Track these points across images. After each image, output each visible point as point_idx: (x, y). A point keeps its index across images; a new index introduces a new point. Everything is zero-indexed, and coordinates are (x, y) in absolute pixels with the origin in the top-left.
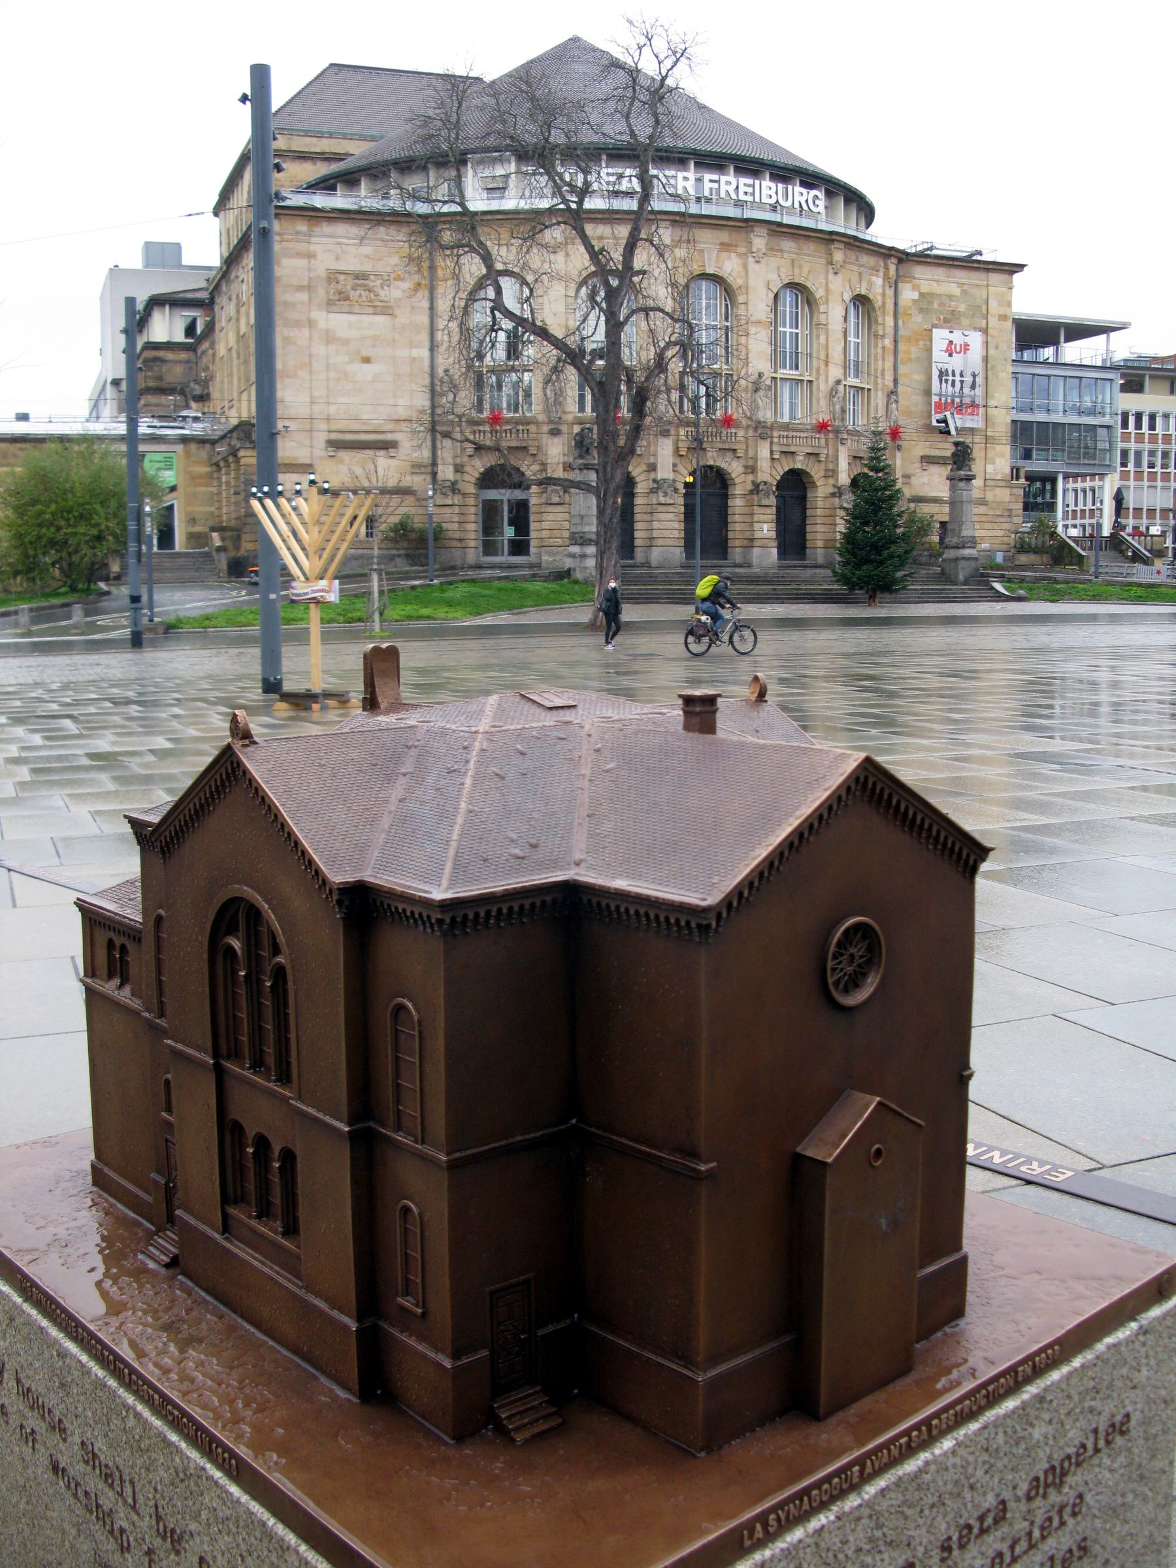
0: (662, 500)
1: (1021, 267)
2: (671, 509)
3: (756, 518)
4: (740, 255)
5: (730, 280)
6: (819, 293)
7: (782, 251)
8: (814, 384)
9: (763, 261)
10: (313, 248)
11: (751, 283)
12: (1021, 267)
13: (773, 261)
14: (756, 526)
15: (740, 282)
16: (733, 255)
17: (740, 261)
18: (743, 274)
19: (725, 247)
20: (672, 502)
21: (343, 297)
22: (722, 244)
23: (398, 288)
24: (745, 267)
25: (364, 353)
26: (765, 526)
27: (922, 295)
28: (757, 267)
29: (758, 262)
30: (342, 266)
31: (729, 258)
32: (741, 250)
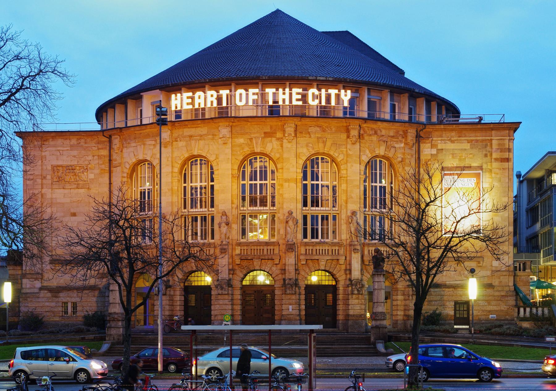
0: (220, 292)
1: (521, 123)
2: (226, 297)
3: (284, 302)
4: (278, 139)
5: (272, 155)
6: (340, 158)
7: (309, 133)
8: (340, 215)
9: (294, 141)
10: (43, 154)
11: (285, 155)
12: (521, 123)
13: (302, 140)
14: (284, 307)
15: (278, 155)
16: (274, 139)
17: (278, 143)
18: (280, 151)
19: (267, 135)
20: (226, 293)
21: (60, 179)
22: (265, 133)
23: (92, 173)
24: (282, 146)
25: (73, 211)
26: (290, 307)
27: (438, 150)
28: (289, 145)
29: (289, 142)
30: (60, 163)
31: (271, 142)
32: (279, 135)
